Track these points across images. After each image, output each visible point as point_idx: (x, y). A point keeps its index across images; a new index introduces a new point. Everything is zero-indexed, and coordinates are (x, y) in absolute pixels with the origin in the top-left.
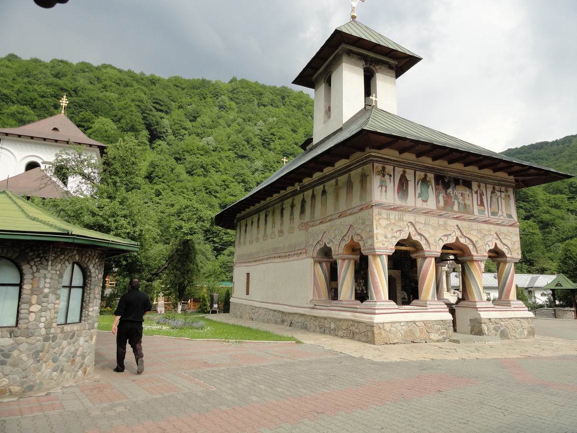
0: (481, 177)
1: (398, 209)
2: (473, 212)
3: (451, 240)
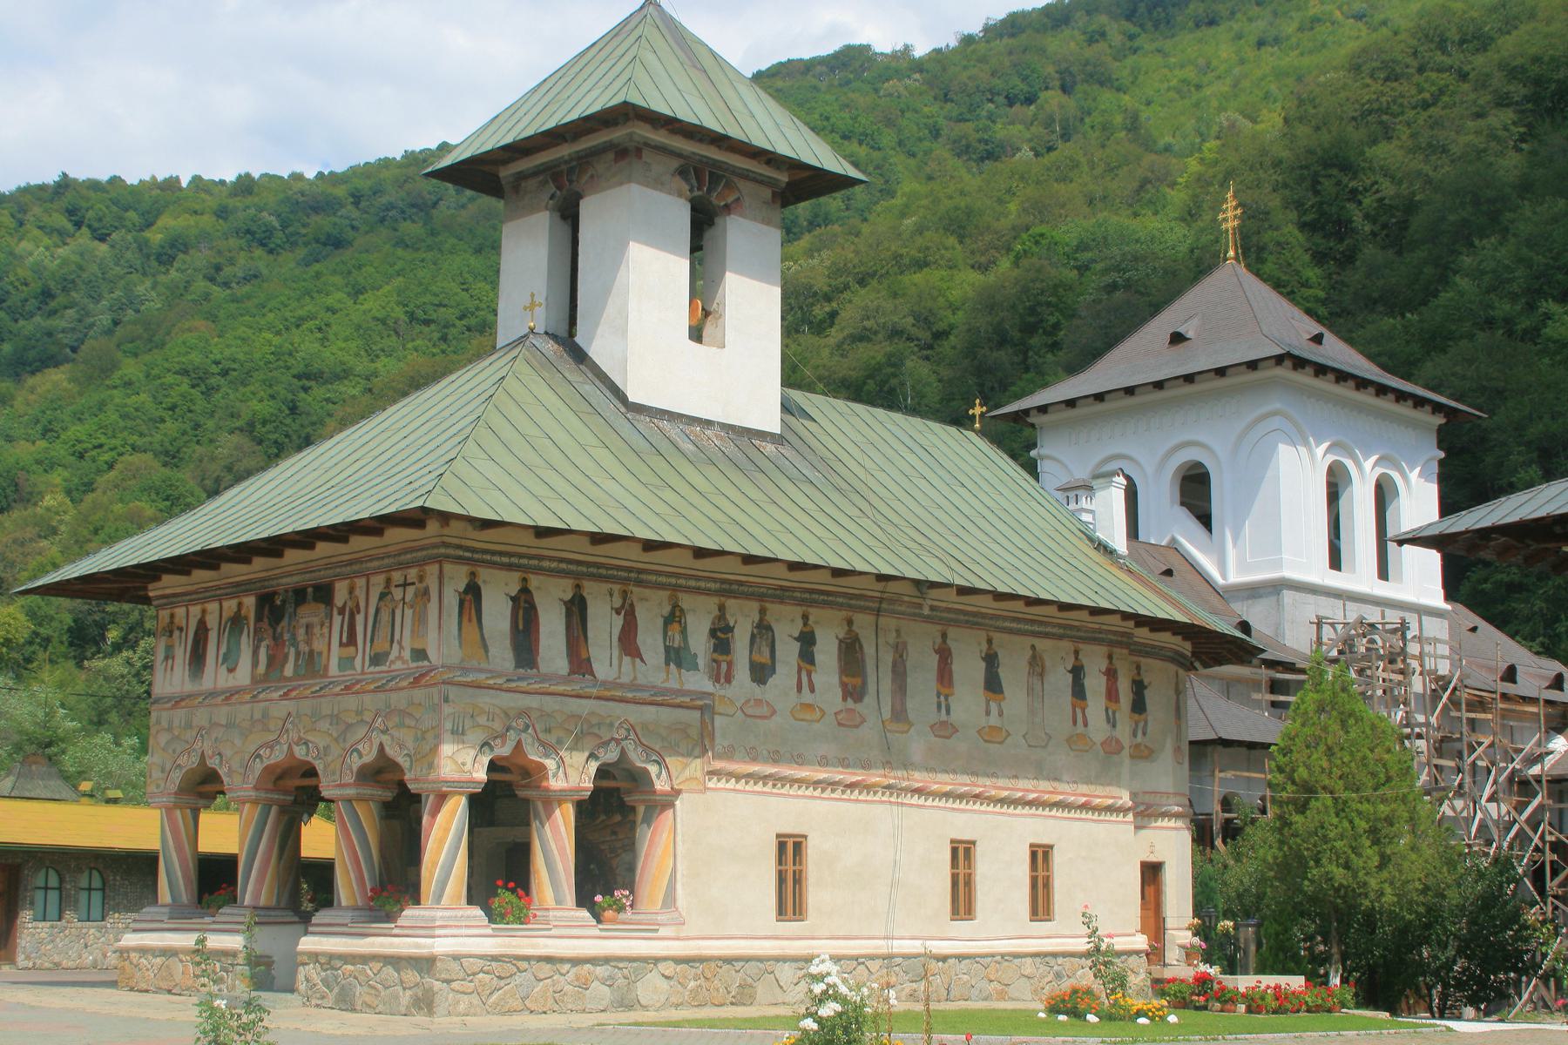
0: (351, 563)
1: (183, 704)
2: (326, 668)
3: (278, 756)
